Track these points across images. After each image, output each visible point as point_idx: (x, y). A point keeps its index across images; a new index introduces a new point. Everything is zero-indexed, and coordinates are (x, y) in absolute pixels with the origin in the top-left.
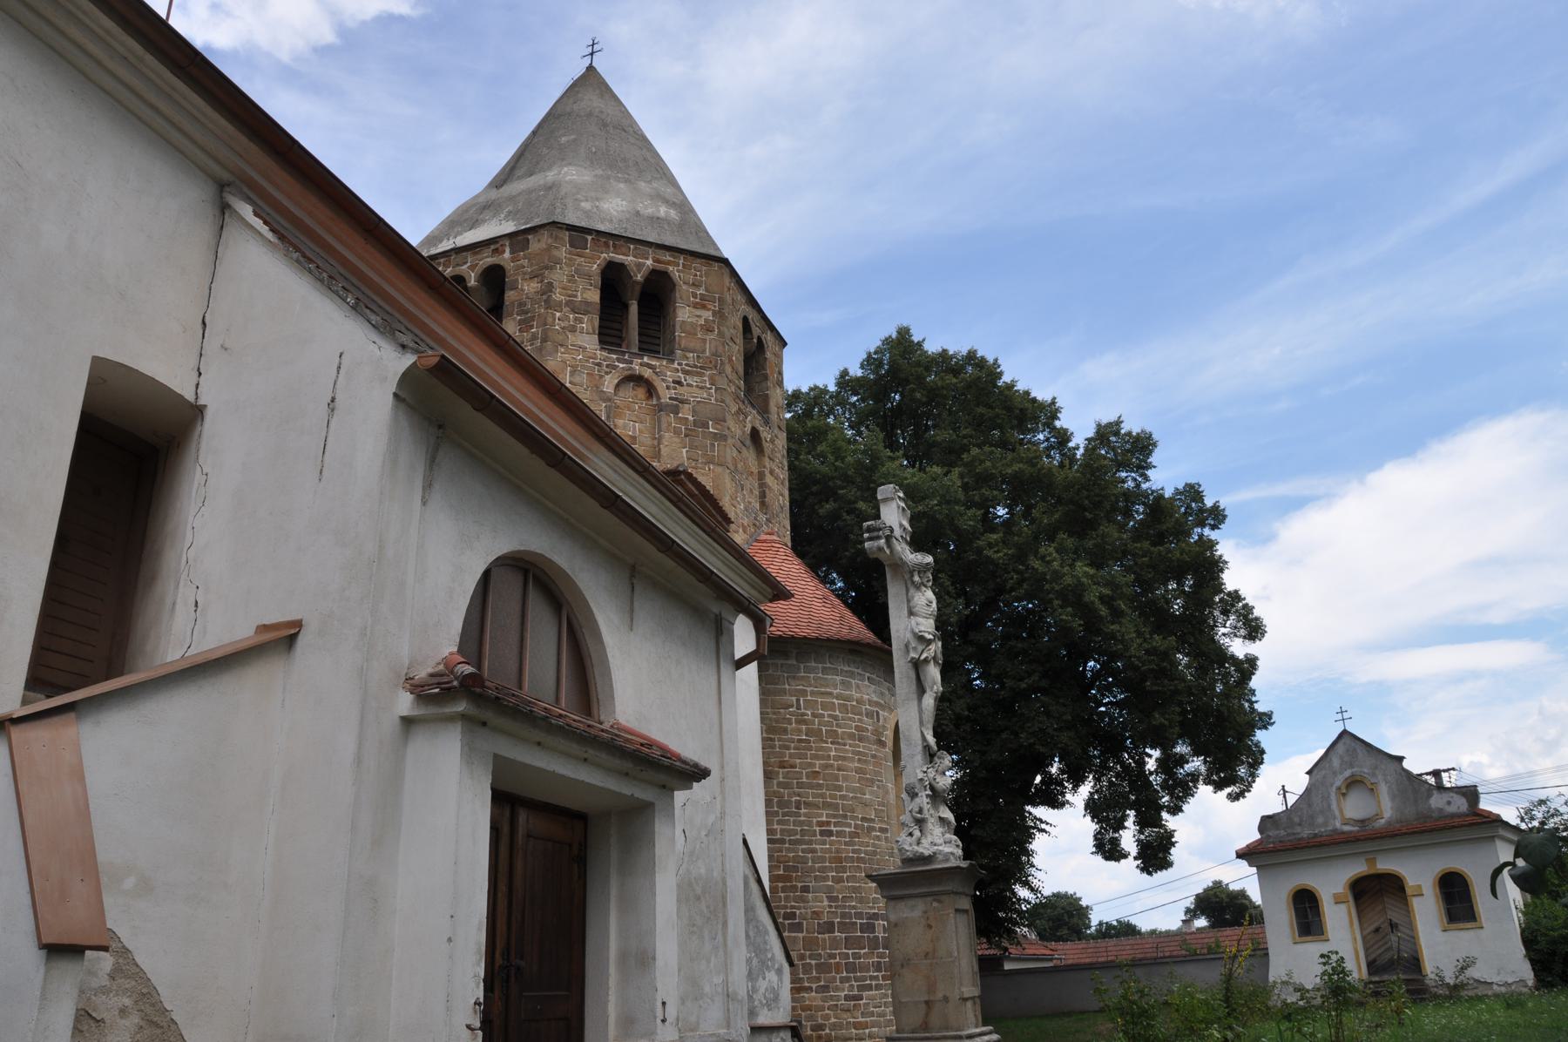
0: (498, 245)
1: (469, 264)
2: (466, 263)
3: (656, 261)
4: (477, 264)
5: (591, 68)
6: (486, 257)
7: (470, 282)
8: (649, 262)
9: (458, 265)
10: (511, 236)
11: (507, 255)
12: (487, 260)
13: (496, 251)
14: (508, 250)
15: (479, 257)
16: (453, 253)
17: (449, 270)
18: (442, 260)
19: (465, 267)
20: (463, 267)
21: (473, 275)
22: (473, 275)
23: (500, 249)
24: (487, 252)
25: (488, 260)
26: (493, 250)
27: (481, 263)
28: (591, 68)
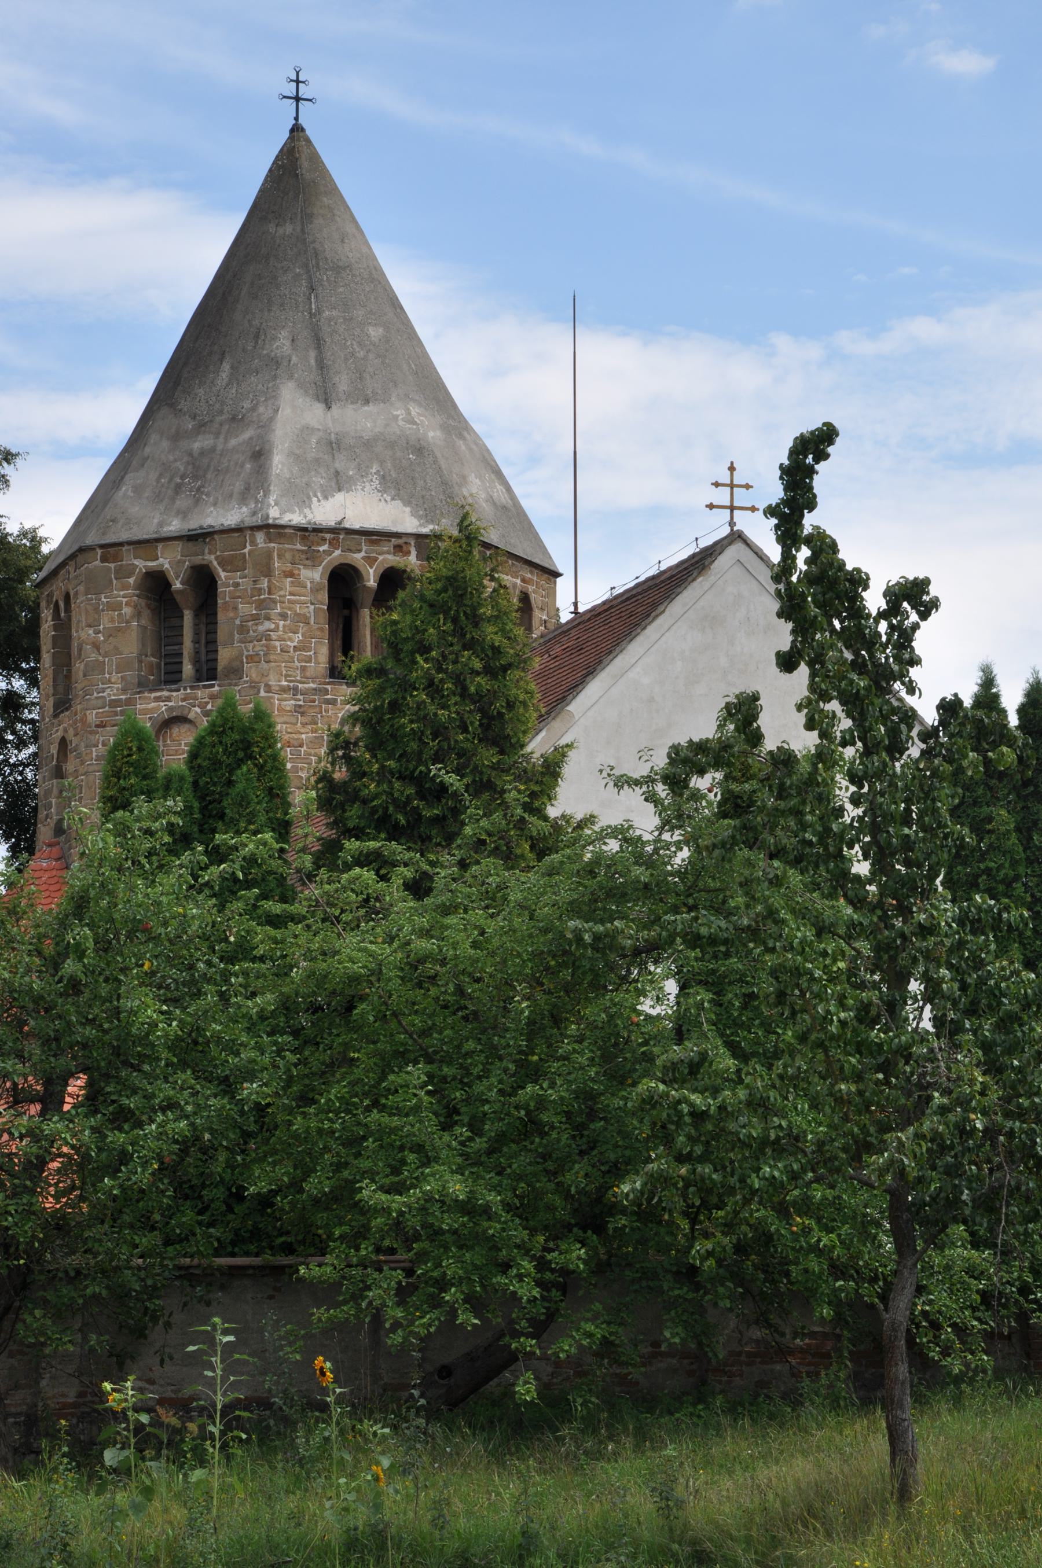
0: (400, 541)
1: (363, 554)
2: (360, 551)
3: (523, 581)
4: (376, 559)
5: (297, 130)
6: (388, 553)
7: (369, 580)
8: (518, 581)
9: (350, 551)
10: (418, 536)
11: (413, 558)
12: (389, 559)
13: (398, 549)
14: (414, 553)
15: (376, 548)
16: (343, 533)
17: (337, 553)
18: (328, 536)
19: (358, 556)
20: (355, 555)
21: (371, 571)
22: (371, 571)
23: (405, 548)
24: (387, 546)
25: (390, 557)
26: (395, 547)
27: (381, 558)
28: (297, 130)
